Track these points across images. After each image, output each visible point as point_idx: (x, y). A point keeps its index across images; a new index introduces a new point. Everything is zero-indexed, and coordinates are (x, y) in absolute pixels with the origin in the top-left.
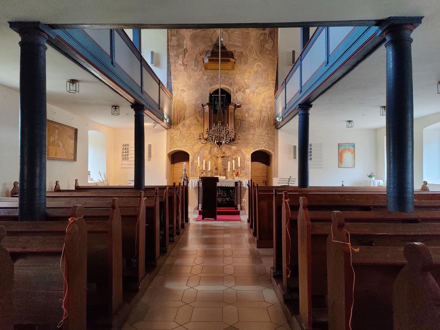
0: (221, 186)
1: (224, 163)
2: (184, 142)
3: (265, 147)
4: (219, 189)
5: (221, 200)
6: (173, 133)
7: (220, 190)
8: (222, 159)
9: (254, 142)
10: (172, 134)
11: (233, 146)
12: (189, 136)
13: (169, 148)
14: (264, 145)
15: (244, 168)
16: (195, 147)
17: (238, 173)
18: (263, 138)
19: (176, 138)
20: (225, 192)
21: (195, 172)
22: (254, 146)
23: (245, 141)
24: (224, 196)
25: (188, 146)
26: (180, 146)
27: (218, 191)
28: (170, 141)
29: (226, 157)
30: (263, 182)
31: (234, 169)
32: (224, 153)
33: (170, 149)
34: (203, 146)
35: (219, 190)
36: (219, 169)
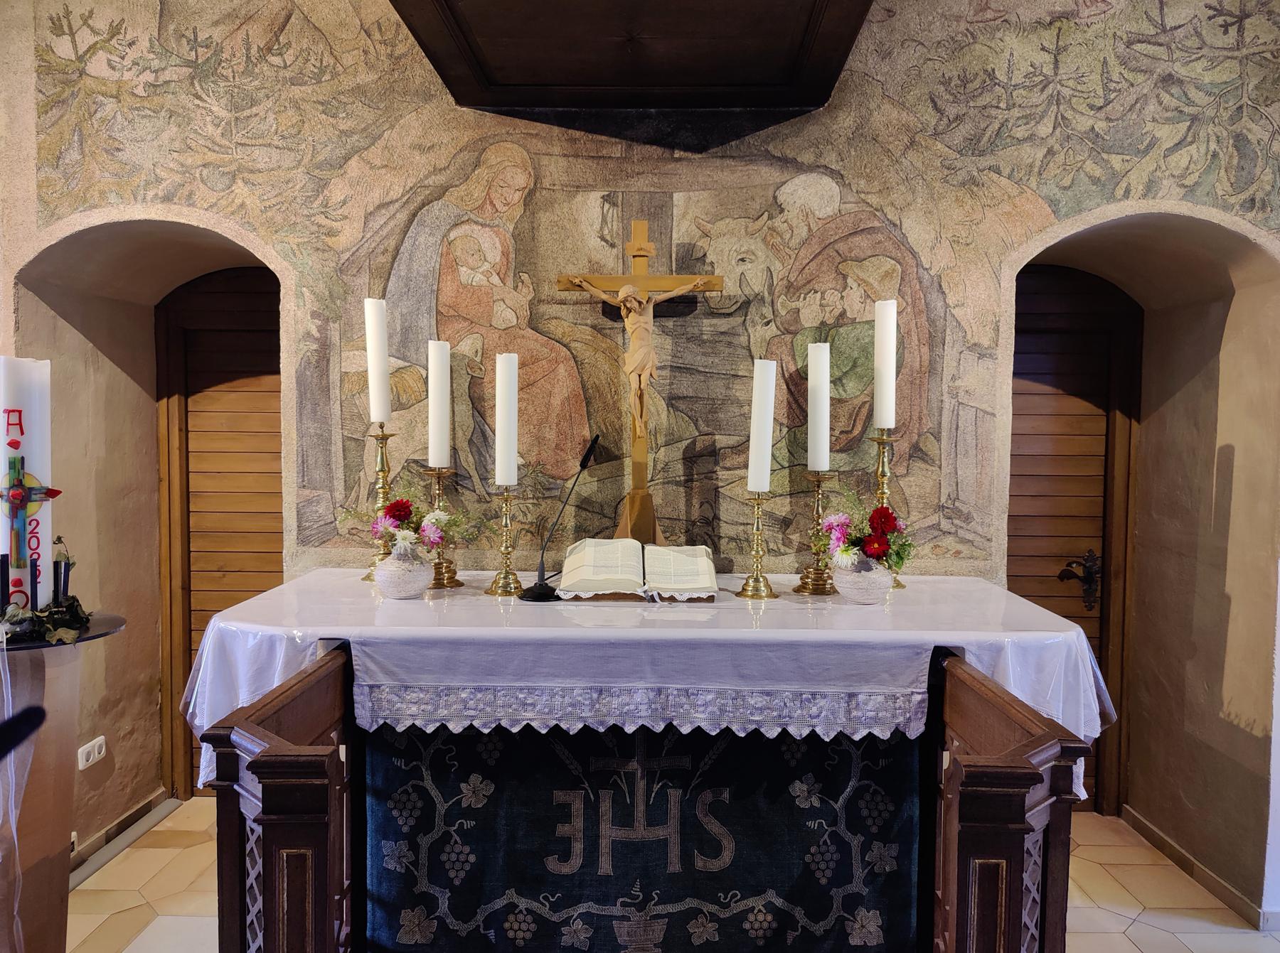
0: (659, 727)
1: (686, 386)
2: (210, 128)
3: (1190, 192)
4: (634, 765)
5: (659, 930)
6: (77, 11)
7: (641, 785)
8: (665, 331)
9: (1061, 122)
10: (57, 30)
11: (803, 177)
12: (262, 58)
13: (34, 205)
14: (1181, 159)
15: (930, 446)
16: (337, 192)
17: (884, 521)
18: (1180, 70)
19: (106, 72)
20: (715, 810)
21: (348, 488)
22: (1053, 169)
23: (952, 111)
24: (700, 863)
25: (258, 178)
26: (159, 180)
27: (616, 786)
28: (43, 109)
29: (713, 314)
30: (1065, 576)
31: (821, 457)
32: (690, 260)
33: (50, 214)
34: (440, 179)
35: (631, 778)
36: (634, 452)
